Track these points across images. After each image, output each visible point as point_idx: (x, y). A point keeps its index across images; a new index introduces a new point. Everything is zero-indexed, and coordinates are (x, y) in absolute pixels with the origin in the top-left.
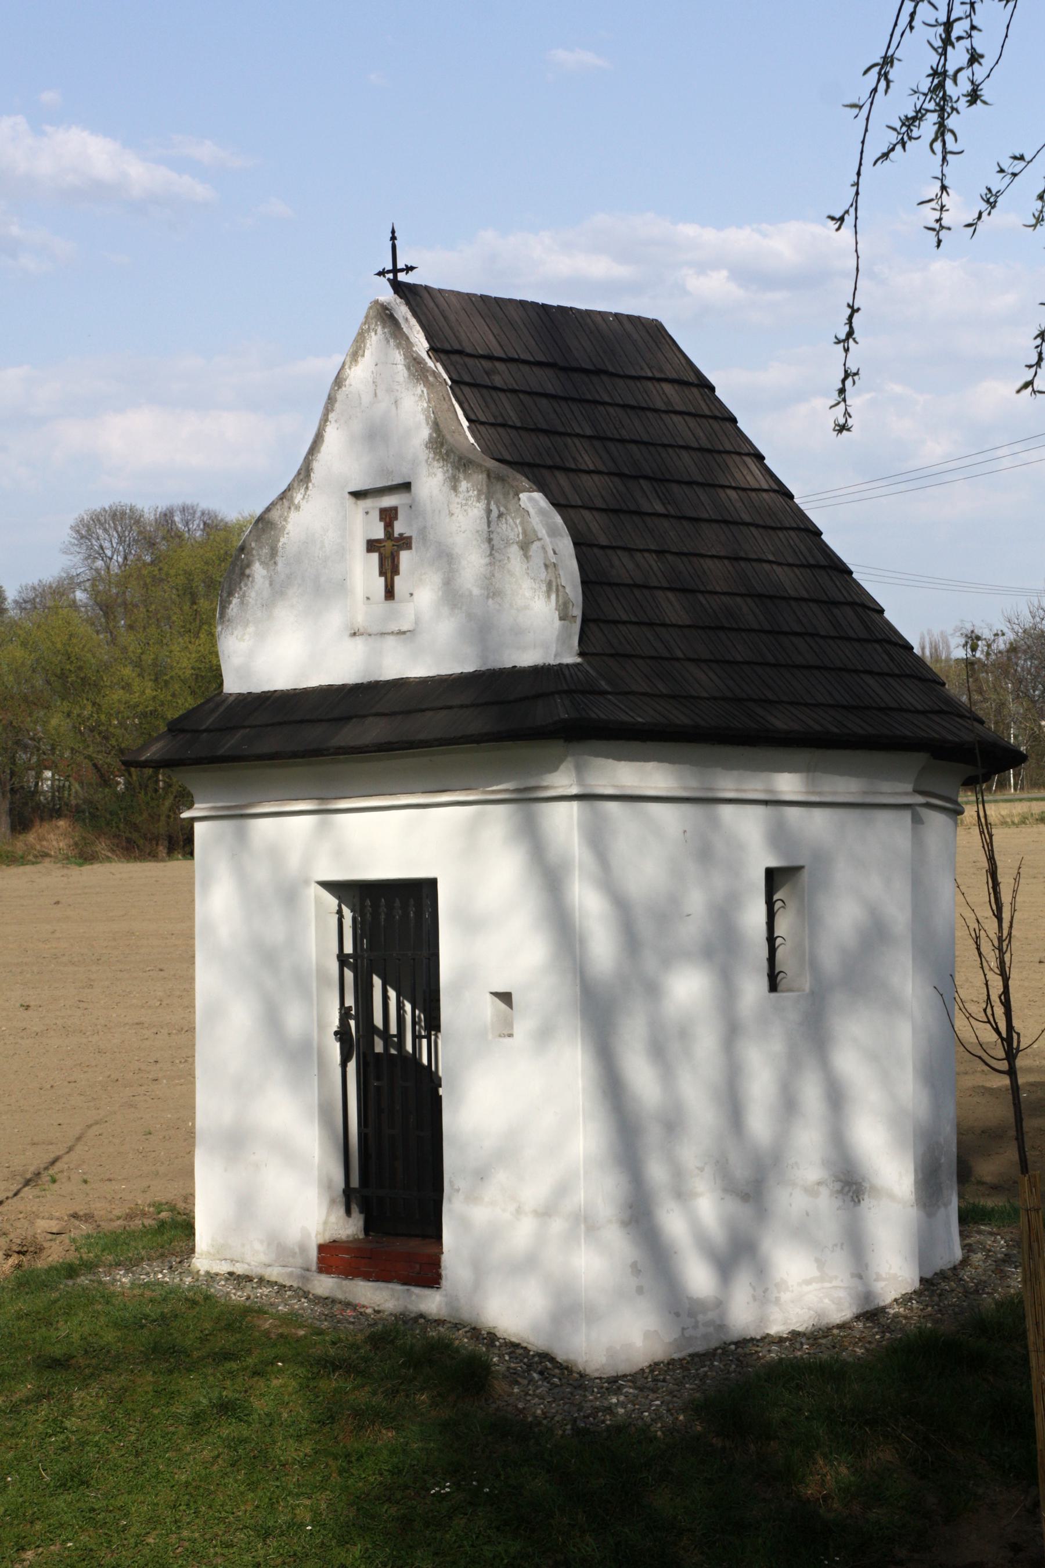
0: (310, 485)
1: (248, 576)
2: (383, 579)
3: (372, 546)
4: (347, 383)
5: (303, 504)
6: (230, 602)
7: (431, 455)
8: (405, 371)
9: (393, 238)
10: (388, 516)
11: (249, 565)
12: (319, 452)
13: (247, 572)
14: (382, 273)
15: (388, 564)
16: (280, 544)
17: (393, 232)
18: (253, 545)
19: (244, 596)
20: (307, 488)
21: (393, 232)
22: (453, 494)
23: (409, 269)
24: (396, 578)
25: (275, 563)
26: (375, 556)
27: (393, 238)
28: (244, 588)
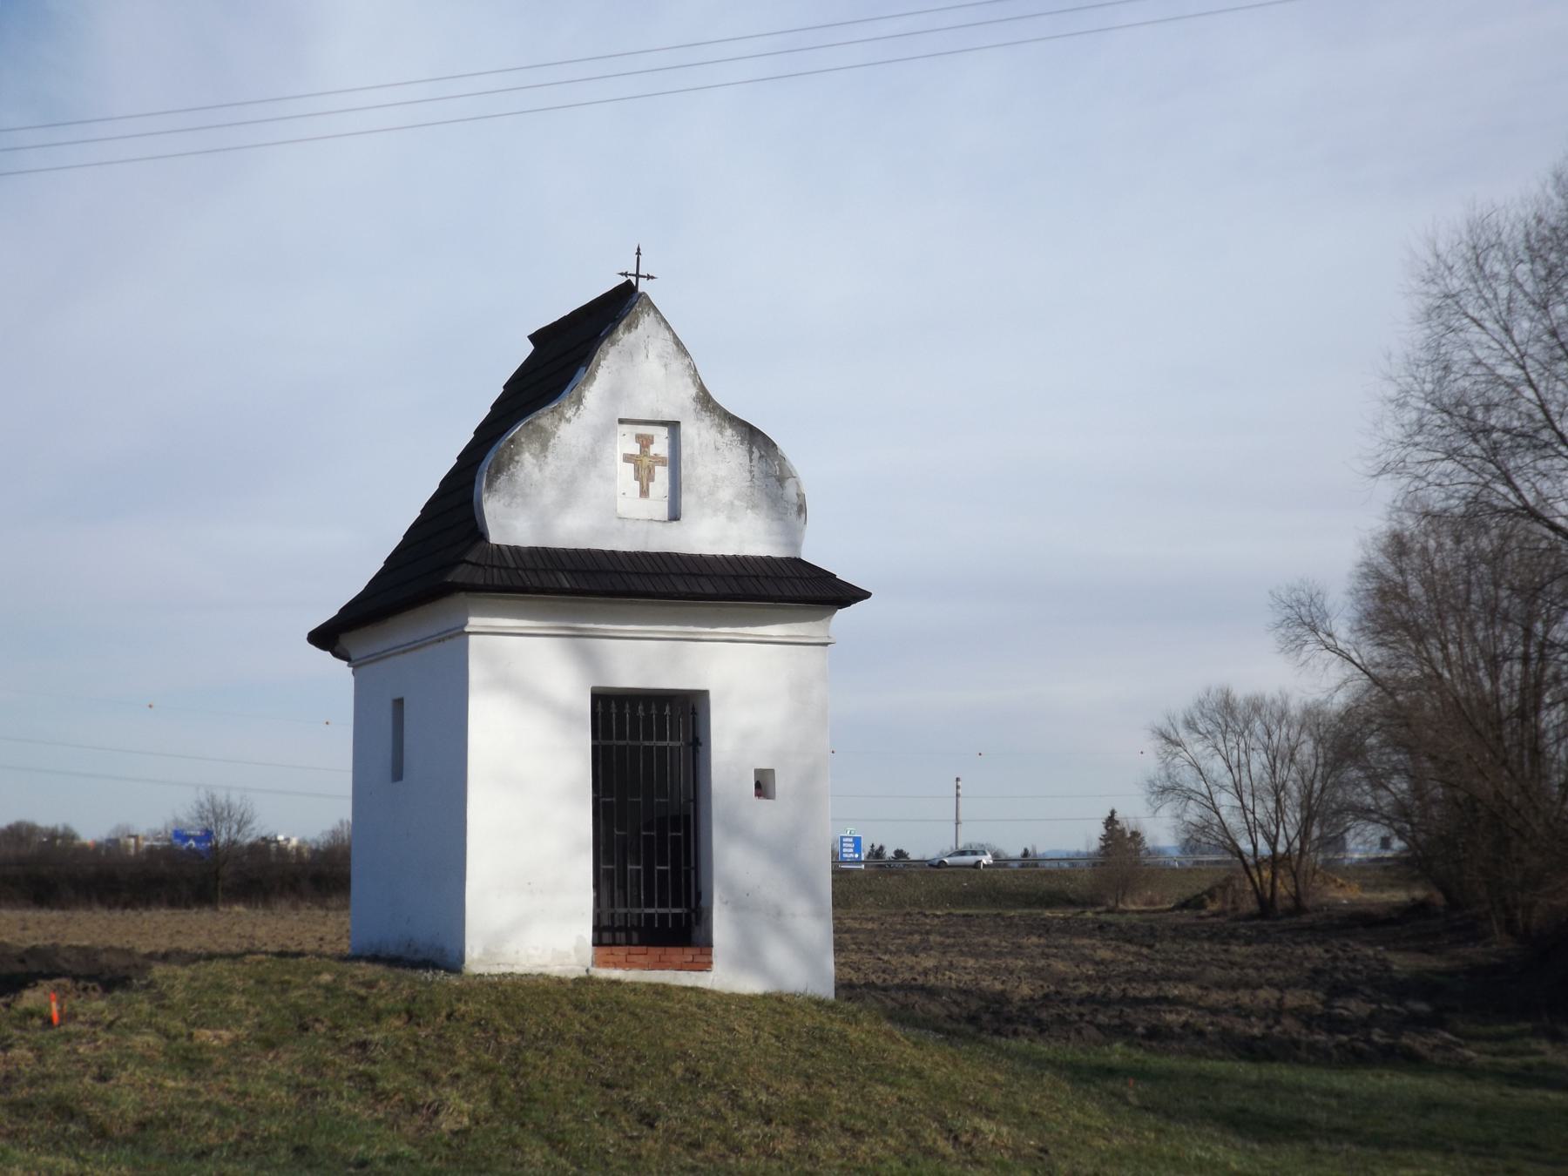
0: (582, 407)
1: (518, 462)
2: (638, 483)
3: (628, 458)
4: (620, 343)
5: (574, 419)
6: (498, 478)
7: (699, 407)
8: (675, 347)
9: (638, 253)
10: (645, 442)
11: (518, 453)
12: (591, 385)
13: (517, 458)
14: (626, 274)
15: (644, 473)
16: (551, 444)
17: (639, 249)
18: (523, 440)
19: (513, 474)
20: (578, 409)
21: (639, 249)
22: (719, 436)
23: (649, 277)
24: (651, 484)
25: (545, 456)
26: (631, 467)
27: (638, 253)
28: (512, 470)
